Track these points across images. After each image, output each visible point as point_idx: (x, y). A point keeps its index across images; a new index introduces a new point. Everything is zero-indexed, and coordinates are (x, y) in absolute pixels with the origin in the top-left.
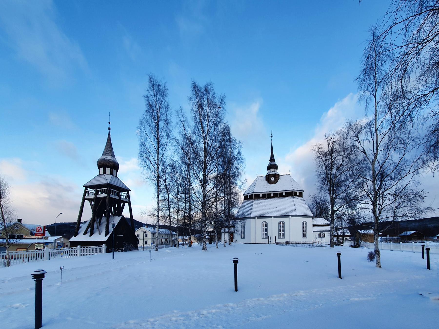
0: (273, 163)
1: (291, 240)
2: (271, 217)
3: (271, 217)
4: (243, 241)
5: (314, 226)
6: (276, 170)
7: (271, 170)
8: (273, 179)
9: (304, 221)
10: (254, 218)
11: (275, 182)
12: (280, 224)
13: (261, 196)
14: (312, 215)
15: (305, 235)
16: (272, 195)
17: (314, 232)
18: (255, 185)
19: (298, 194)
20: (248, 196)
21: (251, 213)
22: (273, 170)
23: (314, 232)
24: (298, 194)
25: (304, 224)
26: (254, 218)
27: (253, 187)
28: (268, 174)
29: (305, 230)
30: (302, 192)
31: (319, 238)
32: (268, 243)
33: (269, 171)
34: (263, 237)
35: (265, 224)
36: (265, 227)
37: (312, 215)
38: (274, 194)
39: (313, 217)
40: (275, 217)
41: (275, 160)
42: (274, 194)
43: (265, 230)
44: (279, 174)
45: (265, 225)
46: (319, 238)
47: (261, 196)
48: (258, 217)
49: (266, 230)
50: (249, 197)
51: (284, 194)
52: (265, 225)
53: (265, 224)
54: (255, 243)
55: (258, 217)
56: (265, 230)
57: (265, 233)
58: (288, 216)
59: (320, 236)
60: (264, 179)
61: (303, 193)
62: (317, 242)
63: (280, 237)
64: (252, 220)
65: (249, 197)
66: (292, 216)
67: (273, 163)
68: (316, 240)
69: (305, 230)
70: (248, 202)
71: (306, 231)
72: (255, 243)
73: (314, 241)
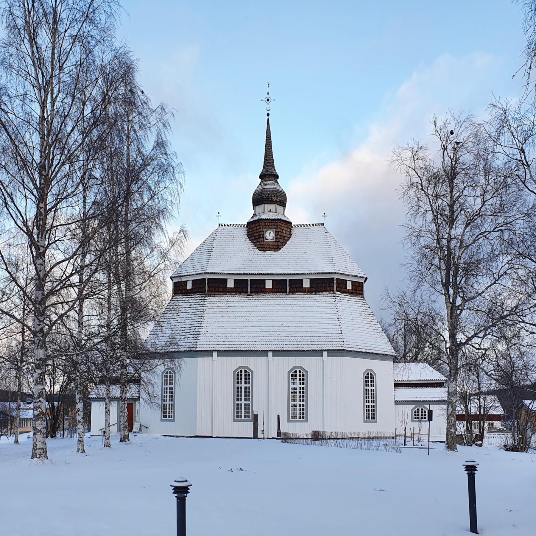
0: (270, 185)
1: (329, 429)
2: (264, 353)
3: (264, 353)
4: (169, 427)
5: (397, 385)
6: (280, 208)
7: (266, 206)
8: (270, 235)
10: (208, 353)
11: (276, 246)
12: (294, 376)
13: (231, 284)
14: (392, 352)
16: (269, 285)
17: (397, 403)
18: (211, 250)
19: (349, 286)
21: (197, 336)
22: (272, 207)
23: (397, 403)
24: (349, 286)
26: (208, 353)
27: (205, 257)
28: (256, 218)
30: (362, 281)
31: (413, 421)
32: (256, 437)
33: (259, 208)
34: (237, 416)
35: (243, 373)
36: (243, 385)
37: (392, 352)
38: (273, 281)
39: (396, 360)
40: (278, 353)
41: (277, 177)
42: (273, 281)
43: (243, 394)
44: (290, 220)
45: (243, 377)
46: (413, 421)
47: (231, 284)
48: (222, 353)
51: (306, 284)
52: (243, 377)
53: (243, 373)
54: (211, 437)
55: (222, 353)
56: (243, 394)
57: (243, 402)
58: (318, 353)
59: (417, 416)
60: (243, 233)
61: (365, 285)
62: (408, 433)
63: (291, 418)
64: (200, 360)
66: (332, 353)
67: (270, 185)
68: (405, 430)
70: (184, 302)
71: (373, 402)
72: (211, 437)
73: (401, 431)
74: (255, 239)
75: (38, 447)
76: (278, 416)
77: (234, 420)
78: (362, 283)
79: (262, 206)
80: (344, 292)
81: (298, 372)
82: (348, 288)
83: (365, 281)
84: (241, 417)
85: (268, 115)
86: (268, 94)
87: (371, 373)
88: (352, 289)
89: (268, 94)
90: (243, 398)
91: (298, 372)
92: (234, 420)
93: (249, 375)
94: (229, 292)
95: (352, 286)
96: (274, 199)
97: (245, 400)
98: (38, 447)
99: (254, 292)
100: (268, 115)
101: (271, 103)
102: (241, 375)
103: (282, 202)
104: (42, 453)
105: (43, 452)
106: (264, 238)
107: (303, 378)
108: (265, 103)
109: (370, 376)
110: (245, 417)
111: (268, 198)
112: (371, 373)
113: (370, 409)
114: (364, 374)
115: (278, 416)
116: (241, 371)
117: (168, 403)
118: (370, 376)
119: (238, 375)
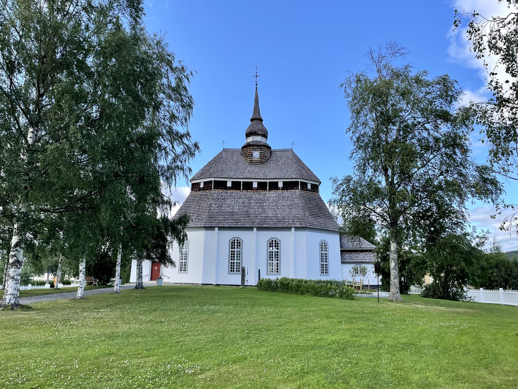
7: (254, 137)
8: (256, 154)
9: (322, 240)
15: (324, 269)
19: (309, 187)
20: (200, 183)
24: (309, 187)
25: (324, 246)
29: (324, 258)
30: (318, 184)
38: (258, 183)
41: (261, 120)
42: (258, 183)
45: (236, 244)
49: (239, 254)
50: (202, 186)
52: (236, 244)
56: (236, 255)
65: (202, 186)
69: (324, 258)
75: (9, 293)
76: (259, 270)
78: (318, 185)
79: (252, 137)
80: (306, 190)
81: (274, 241)
82: (308, 188)
83: (320, 184)
84: (234, 271)
85: (256, 85)
86: (257, 73)
87: (325, 243)
88: (311, 189)
89: (257, 73)
90: (235, 258)
91: (274, 241)
93: (240, 243)
94: (228, 189)
95: (311, 187)
96: (260, 133)
97: (237, 260)
98: (9, 293)
100: (256, 85)
101: (258, 78)
102: (234, 243)
103: (265, 136)
104: (12, 298)
105: (14, 298)
106: (252, 156)
107: (277, 245)
108: (254, 78)
109: (324, 244)
110: (237, 271)
112: (325, 243)
113: (324, 266)
114: (320, 243)
115: (259, 270)
116: (234, 240)
117: (184, 261)
118: (324, 244)
119: (232, 243)
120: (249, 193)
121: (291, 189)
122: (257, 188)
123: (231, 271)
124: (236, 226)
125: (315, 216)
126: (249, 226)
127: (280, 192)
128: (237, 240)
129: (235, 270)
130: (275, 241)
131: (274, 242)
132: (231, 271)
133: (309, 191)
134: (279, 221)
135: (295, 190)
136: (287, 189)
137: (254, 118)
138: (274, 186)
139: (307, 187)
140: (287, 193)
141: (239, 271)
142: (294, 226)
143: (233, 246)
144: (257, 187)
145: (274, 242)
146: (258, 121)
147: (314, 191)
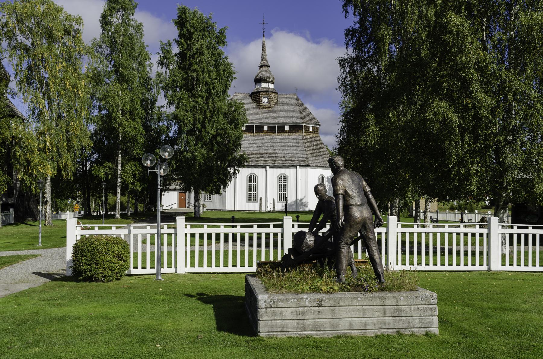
8: (265, 100)
9: (321, 175)
19: (311, 129)
24: (311, 129)
35: (252, 177)
52: (252, 179)
74: (257, 102)
77: (247, 202)
80: (308, 133)
84: (251, 200)
92: (247, 202)
96: (268, 79)
99: (258, 132)
102: (251, 178)
110: (253, 200)
111: (264, 79)
116: (251, 176)
120: (262, 136)
121: (296, 132)
122: (268, 130)
123: (249, 200)
124: (253, 164)
125: (316, 155)
126: (263, 164)
127: (286, 135)
128: (254, 176)
129: (252, 199)
130: (284, 176)
131: (283, 177)
132: (249, 200)
133: (310, 133)
134: (286, 160)
135: (299, 133)
136: (292, 132)
137: (263, 65)
138: (281, 129)
139: (309, 130)
140: (293, 136)
141: (255, 200)
142: (299, 164)
143: (250, 180)
144: (267, 130)
145: (283, 177)
146: (266, 68)
147: (315, 133)
